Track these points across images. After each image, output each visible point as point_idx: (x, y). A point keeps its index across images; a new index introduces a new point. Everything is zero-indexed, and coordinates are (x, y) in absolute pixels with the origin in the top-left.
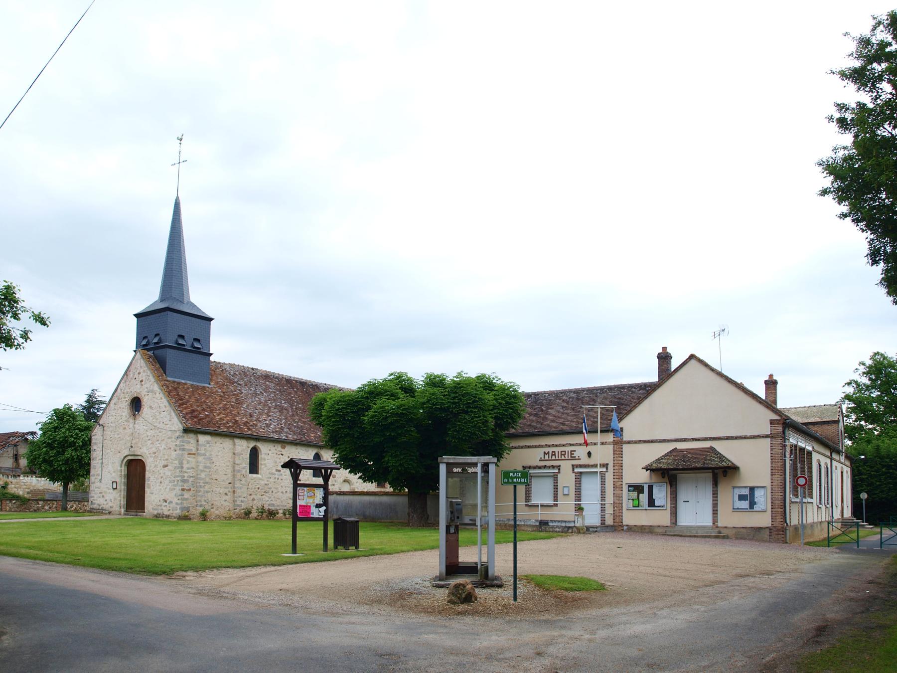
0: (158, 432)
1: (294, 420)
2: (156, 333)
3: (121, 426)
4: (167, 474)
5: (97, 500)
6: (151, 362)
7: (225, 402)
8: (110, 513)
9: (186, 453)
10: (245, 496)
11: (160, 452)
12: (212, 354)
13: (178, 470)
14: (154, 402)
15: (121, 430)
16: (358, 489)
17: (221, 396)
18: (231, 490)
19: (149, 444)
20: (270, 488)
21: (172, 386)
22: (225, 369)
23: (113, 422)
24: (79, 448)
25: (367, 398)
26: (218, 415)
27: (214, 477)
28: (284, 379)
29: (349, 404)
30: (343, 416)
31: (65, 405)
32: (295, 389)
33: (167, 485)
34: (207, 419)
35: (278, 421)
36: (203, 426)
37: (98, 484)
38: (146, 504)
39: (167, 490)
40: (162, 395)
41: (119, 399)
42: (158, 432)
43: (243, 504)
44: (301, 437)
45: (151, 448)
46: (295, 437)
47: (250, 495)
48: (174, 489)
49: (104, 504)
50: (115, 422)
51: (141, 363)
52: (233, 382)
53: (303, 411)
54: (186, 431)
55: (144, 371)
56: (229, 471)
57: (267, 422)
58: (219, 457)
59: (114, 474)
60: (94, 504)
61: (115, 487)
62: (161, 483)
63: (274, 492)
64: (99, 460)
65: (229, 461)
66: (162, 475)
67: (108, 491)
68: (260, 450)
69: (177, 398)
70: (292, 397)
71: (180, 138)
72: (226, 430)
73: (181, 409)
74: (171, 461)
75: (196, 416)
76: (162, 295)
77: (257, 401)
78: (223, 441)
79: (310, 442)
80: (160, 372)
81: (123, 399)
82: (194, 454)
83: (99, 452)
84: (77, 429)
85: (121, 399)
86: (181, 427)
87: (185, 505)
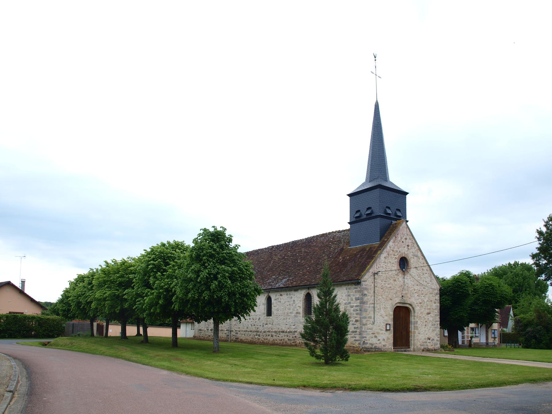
5: (369, 340)
11: (424, 303)
15: (392, 281)
19: (416, 296)
33: (430, 327)
38: (412, 342)
39: (431, 331)
42: (422, 288)
48: (435, 330)
49: (376, 344)
59: (386, 318)
61: (388, 328)
62: (426, 325)
66: (426, 320)
67: (381, 332)
83: (369, 297)
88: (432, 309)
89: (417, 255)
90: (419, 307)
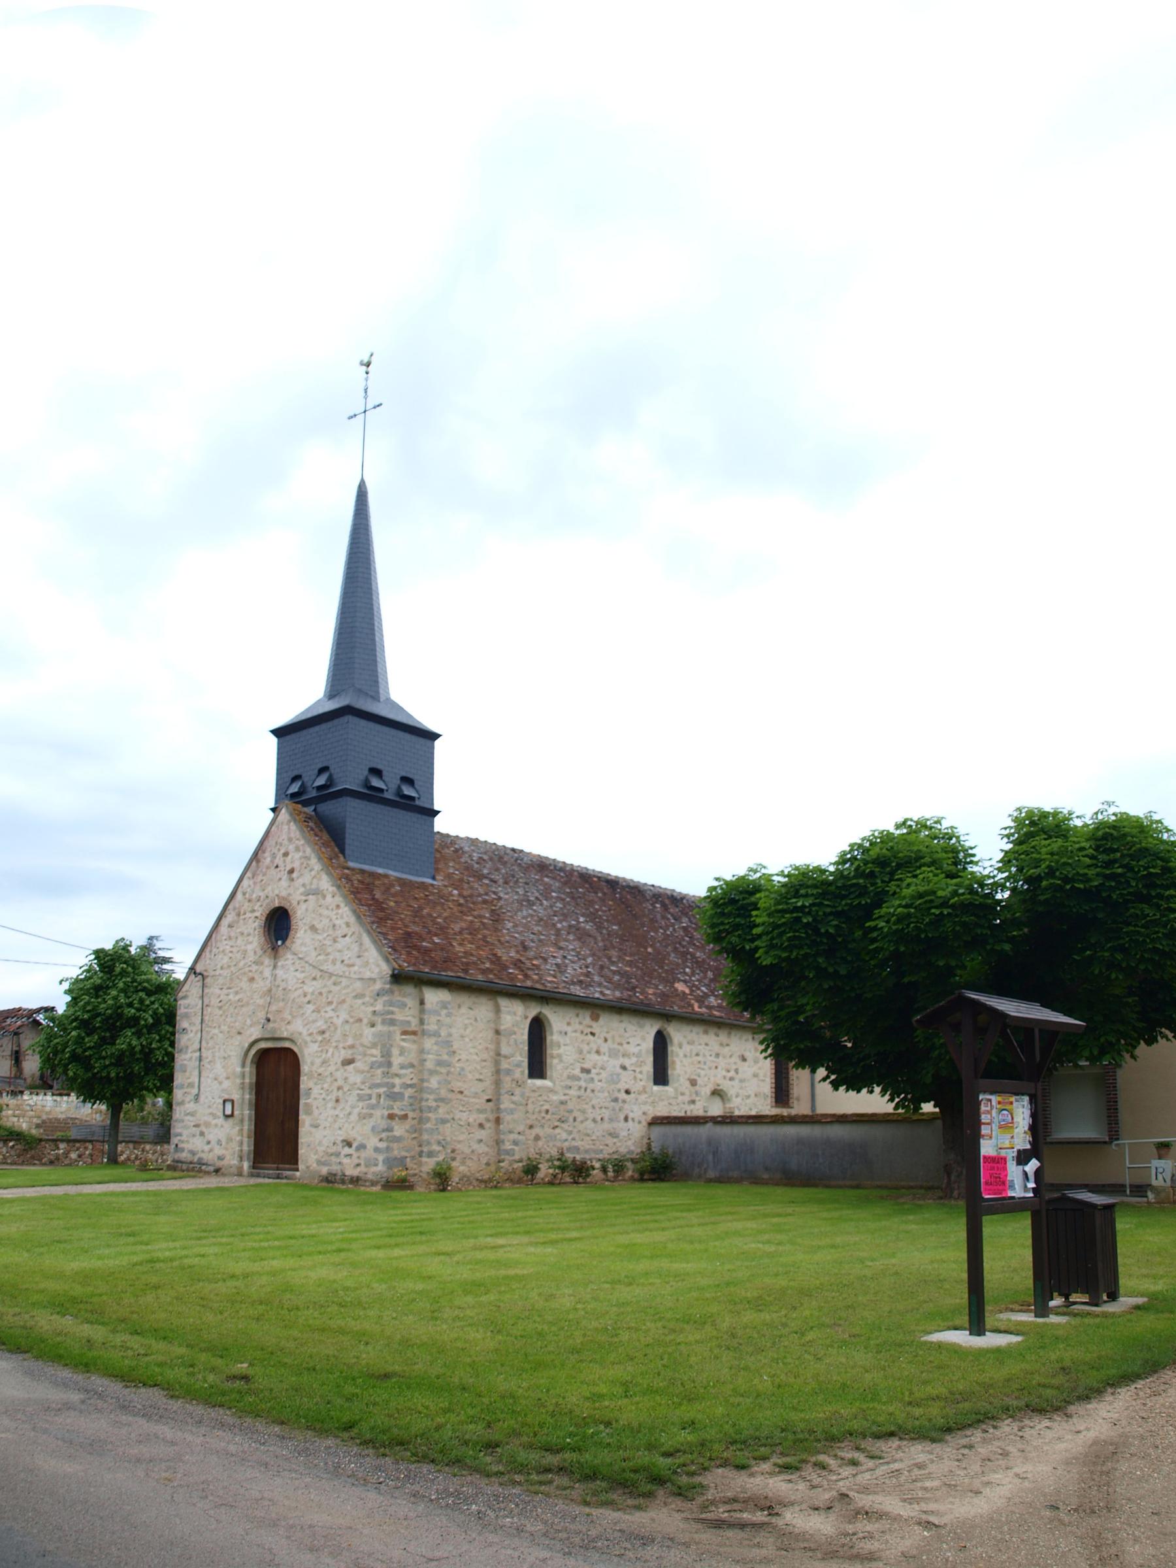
0: (330, 983)
1: (609, 958)
2: (320, 766)
3: (245, 973)
4: (352, 1080)
5: (188, 1142)
6: (312, 829)
7: (470, 918)
8: (217, 1171)
9: (397, 1031)
10: (521, 1128)
11: (336, 1029)
12: (439, 812)
13: (379, 1071)
14: (321, 915)
15: (244, 984)
16: (739, 1110)
17: (460, 905)
18: (492, 1117)
19: (309, 1012)
20: (570, 1111)
21: (359, 881)
22: (461, 848)
23: (225, 966)
24: (145, 1030)
25: (872, 875)
26: (460, 944)
27: (457, 1085)
28: (576, 873)
29: (824, 895)
30: (813, 928)
31: (117, 942)
32: (600, 895)
33: (353, 1107)
34: (439, 953)
35: (579, 959)
36: (434, 967)
37: (190, 1106)
39: (354, 1117)
40: (339, 899)
41: (239, 915)
42: (330, 983)
43: (516, 1148)
44: (630, 996)
45: (314, 1021)
46: (618, 994)
47: (531, 1127)
48: (371, 1116)
49: (203, 1151)
50: (229, 967)
51: (291, 831)
52: (480, 877)
53: (623, 941)
54: (398, 978)
55: (297, 849)
56: (488, 1072)
57: (559, 961)
58: (467, 1040)
59: (226, 1084)
60: (183, 1150)
61: (228, 1112)
62: (337, 1101)
63: (579, 1120)
64: (194, 1051)
65: (487, 1049)
66: (340, 1082)
67: (214, 1122)
68: (550, 1026)
69: (371, 905)
70: (597, 910)
71: (366, 361)
72: (480, 977)
73: (384, 930)
74: (361, 1049)
75: (416, 946)
76: (332, 686)
77: (532, 916)
78: (474, 1003)
79: (648, 1005)
80: (333, 850)
81: (249, 915)
82: (414, 1033)
83: (192, 1035)
84: (141, 990)
85: (245, 914)
86: (386, 969)
87: (396, 1152)
88: (362, 1045)
89: (318, 889)
90: (317, 1044)
